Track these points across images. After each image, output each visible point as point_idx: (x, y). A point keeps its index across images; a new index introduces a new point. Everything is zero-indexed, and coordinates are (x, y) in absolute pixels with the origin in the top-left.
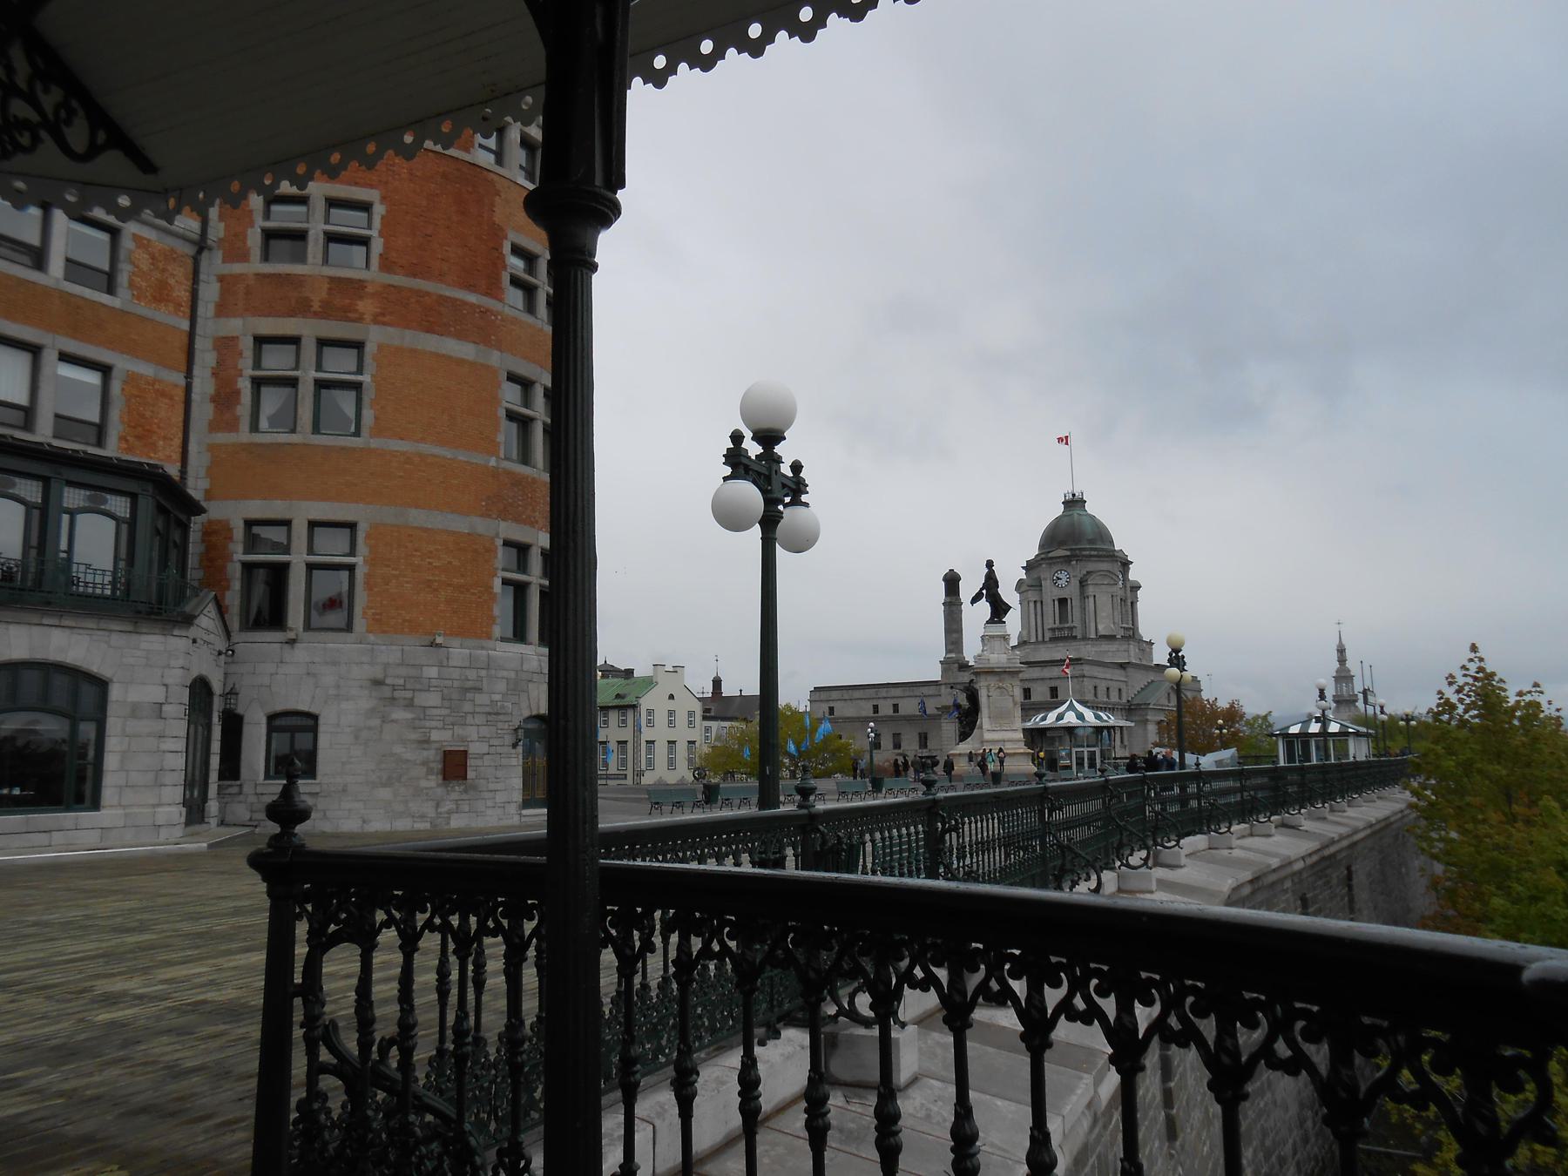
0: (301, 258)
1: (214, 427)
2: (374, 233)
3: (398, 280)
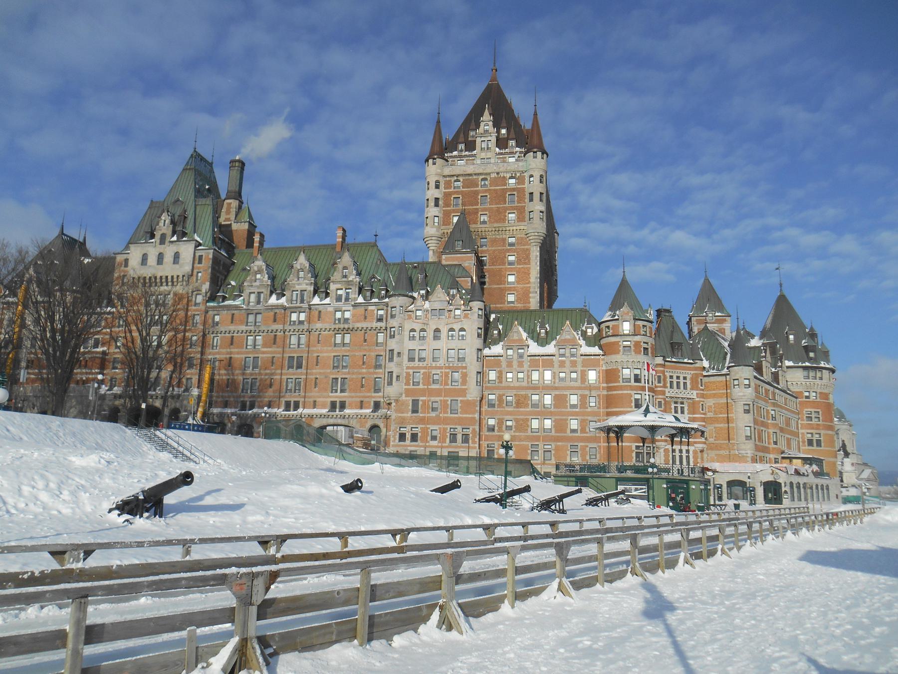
0: (811, 421)
1: (802, 446)
2: (820, 416)
3: (825, 423)
